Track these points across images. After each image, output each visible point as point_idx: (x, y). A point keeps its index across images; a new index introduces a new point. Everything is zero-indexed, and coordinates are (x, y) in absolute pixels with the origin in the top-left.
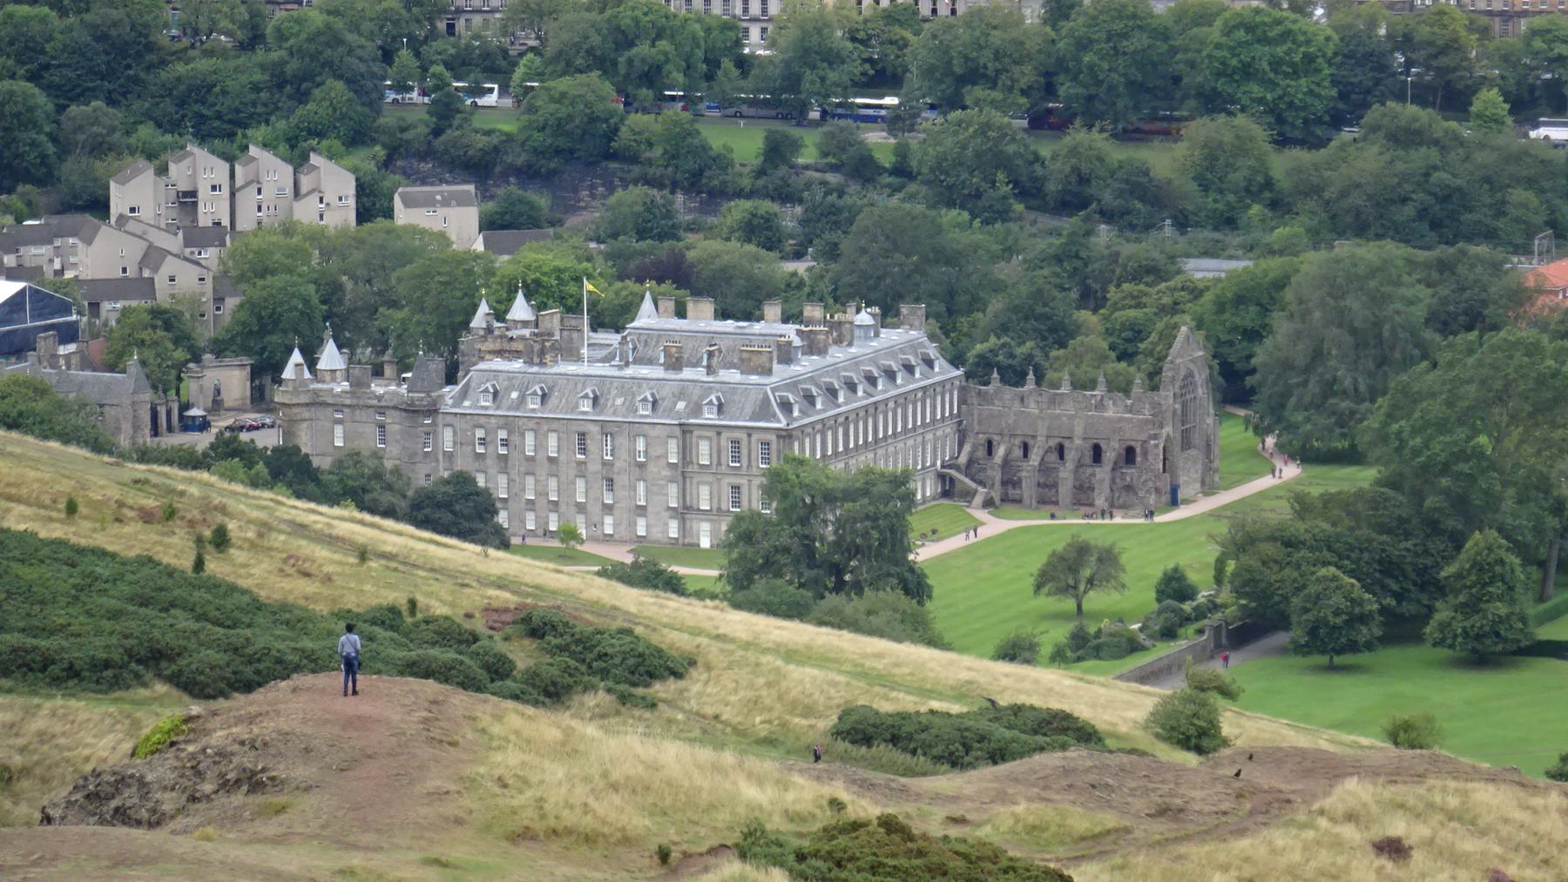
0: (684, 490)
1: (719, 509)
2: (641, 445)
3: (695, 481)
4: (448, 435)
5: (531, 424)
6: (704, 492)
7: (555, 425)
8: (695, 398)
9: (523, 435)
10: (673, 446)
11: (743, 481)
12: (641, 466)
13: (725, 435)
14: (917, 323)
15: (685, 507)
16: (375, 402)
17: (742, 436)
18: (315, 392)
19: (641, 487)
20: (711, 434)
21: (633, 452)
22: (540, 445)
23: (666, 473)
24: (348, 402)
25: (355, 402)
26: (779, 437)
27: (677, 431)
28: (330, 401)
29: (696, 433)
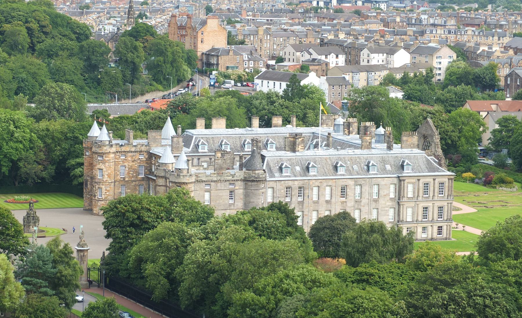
1: (417, 220)
2: (375, 189)
3: (405, 206)
4: (270, 191)
7: (330, 183)
9: (312, 189)
10: (392, 187)
11: (430, 204)
12: (376, 201)
13: (423, 181)
14: (330, 123)
16: (230, 178)
17: (430, 180)
20: (414, 180)
21: (371, 194)
23: (390, 203)
24: (215, 179)
25: (219, 178)
26: (449, 179)
27: (396, 181)
28: (204, 179)
29: (407, 181)
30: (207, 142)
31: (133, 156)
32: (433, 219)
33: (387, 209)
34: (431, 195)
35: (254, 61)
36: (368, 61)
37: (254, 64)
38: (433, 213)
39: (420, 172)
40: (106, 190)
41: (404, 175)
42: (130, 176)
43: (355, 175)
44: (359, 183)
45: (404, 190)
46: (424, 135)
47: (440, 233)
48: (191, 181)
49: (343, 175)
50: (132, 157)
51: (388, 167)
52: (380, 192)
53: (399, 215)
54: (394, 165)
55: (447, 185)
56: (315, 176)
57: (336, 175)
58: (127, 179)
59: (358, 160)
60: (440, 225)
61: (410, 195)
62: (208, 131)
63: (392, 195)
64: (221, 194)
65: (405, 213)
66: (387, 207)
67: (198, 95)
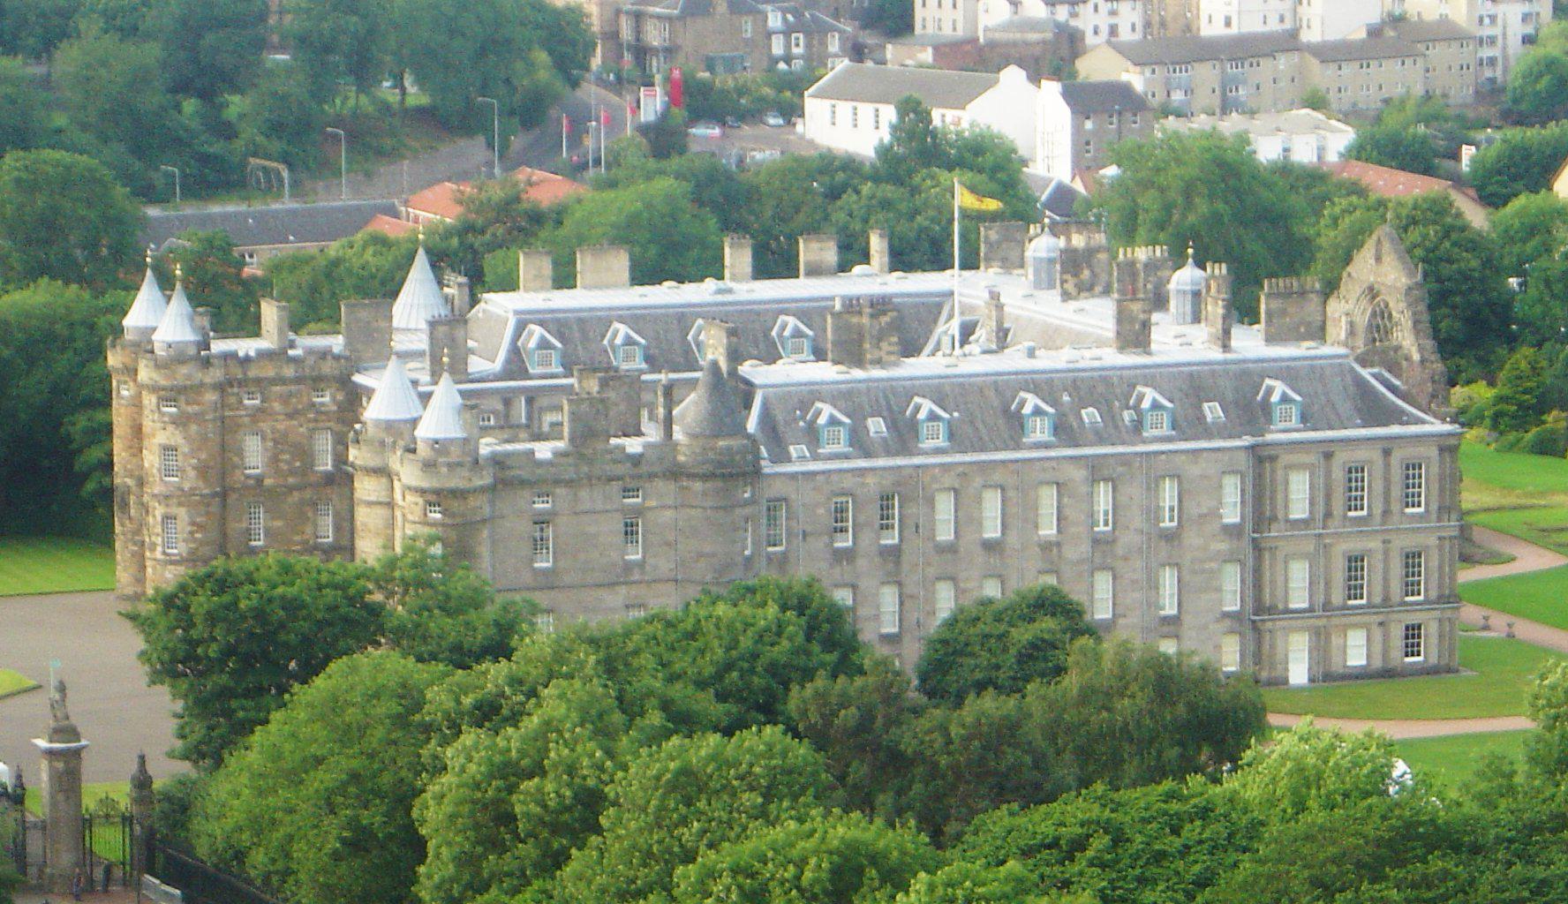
0: (1257, 572)
1: (1327, 606)
2: (1168, 494)
3: (1280, 555)
5: (949, 480)
6: (1299, 574)
7: (997, 477)
8: (1230, 396)
9: (931, 502)
12: (1170, 537)
13: (1342, 458)
15: (1259, 609)
18: (498, 461)
19: (1168, 579)
21: (1153, 513)
22: (966, 518)
23: (1223, 546)
24: (570, 474)
26: (1442, 450)
27: (1243, 461)
28: (524, 474)
29: (1285, 459)
30: (561, 337)
31: (291, 395)
32: (1386, 599)
33: (1213, 565)
34: (1378, 511)
35: (808, 35)
36: (1228, 23)
37: (808, 46)
38: (1382, 577)
39: (1331, 428)
40: (193, 524)
41: (1269, 437)
42: (278, 471)
43: (1092, 445)
44: (1106, 473)
45: (1274, 492)
46: (1371, 289)
47: (1412, 650)
48: (479, 483)
49: (1047, 446)
50: (285, 399)
51: (1212, 411)
52: (1185, 504)
53: (1258, 586)
54: (1236, 403)
55: (1435, 469)
56: (938, 451)
57: (1018, 447)
58: (268, 482)
59: (1100, 389)
60: (1413, 619)
61: (1299, 511)
62: (563, 300)
63: (1232, 516)
64: (592, 529)
65: (1280, 580)
66: (1211, 560)
67: (597, 162)
